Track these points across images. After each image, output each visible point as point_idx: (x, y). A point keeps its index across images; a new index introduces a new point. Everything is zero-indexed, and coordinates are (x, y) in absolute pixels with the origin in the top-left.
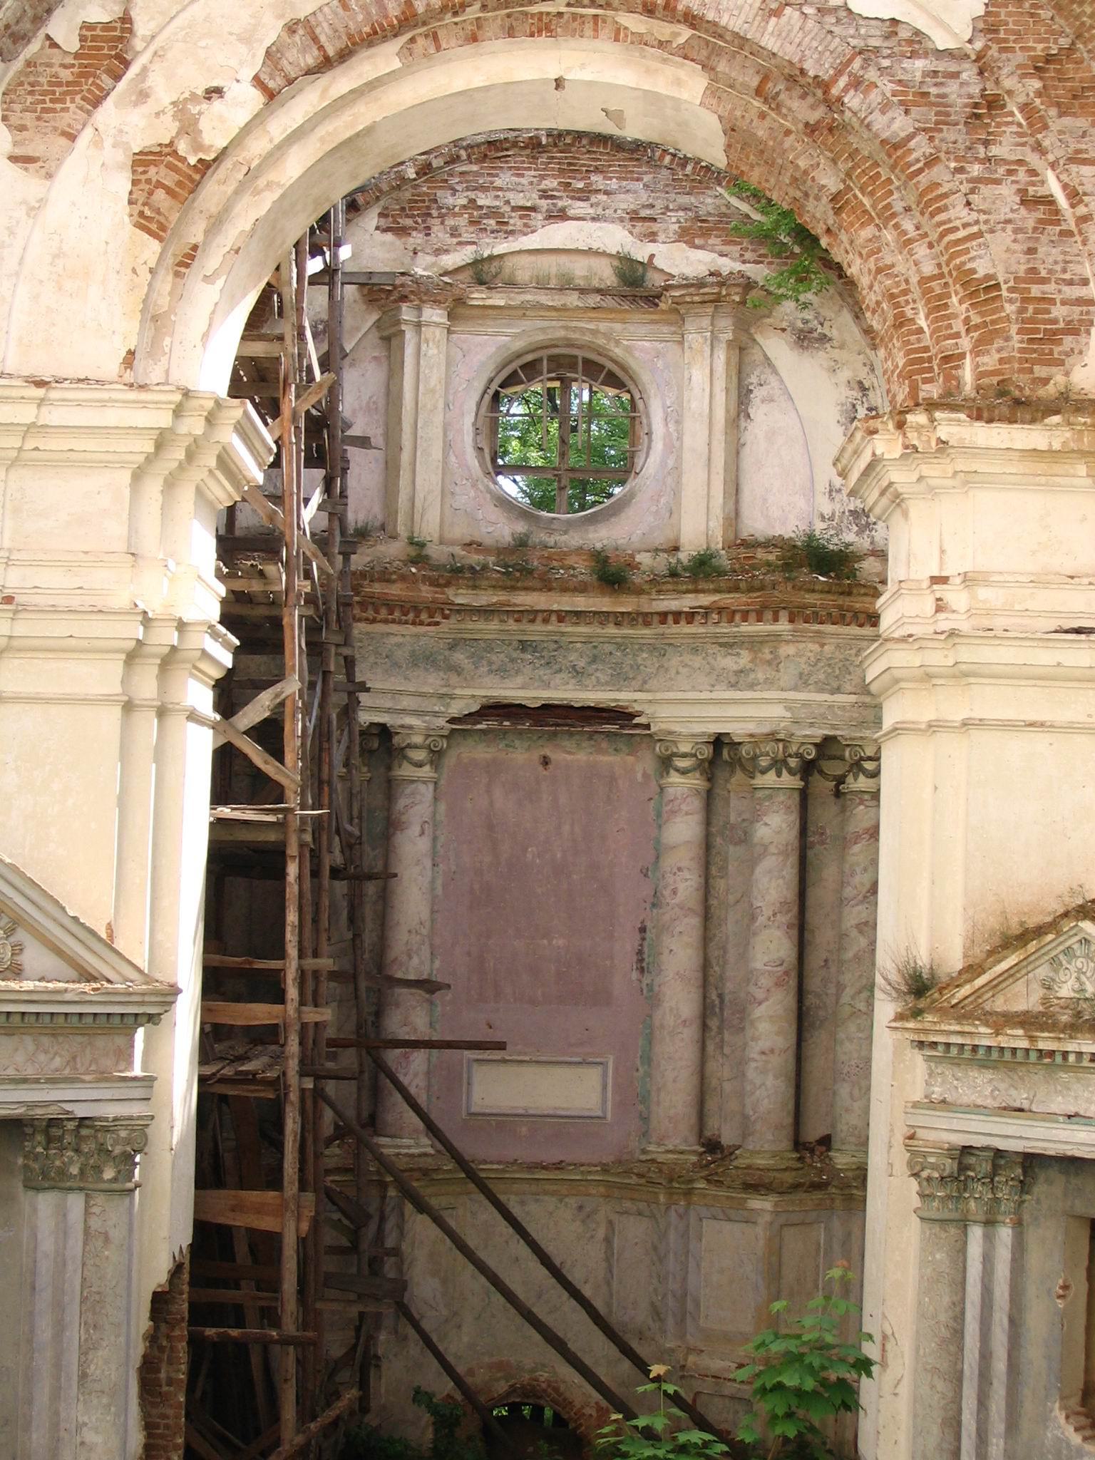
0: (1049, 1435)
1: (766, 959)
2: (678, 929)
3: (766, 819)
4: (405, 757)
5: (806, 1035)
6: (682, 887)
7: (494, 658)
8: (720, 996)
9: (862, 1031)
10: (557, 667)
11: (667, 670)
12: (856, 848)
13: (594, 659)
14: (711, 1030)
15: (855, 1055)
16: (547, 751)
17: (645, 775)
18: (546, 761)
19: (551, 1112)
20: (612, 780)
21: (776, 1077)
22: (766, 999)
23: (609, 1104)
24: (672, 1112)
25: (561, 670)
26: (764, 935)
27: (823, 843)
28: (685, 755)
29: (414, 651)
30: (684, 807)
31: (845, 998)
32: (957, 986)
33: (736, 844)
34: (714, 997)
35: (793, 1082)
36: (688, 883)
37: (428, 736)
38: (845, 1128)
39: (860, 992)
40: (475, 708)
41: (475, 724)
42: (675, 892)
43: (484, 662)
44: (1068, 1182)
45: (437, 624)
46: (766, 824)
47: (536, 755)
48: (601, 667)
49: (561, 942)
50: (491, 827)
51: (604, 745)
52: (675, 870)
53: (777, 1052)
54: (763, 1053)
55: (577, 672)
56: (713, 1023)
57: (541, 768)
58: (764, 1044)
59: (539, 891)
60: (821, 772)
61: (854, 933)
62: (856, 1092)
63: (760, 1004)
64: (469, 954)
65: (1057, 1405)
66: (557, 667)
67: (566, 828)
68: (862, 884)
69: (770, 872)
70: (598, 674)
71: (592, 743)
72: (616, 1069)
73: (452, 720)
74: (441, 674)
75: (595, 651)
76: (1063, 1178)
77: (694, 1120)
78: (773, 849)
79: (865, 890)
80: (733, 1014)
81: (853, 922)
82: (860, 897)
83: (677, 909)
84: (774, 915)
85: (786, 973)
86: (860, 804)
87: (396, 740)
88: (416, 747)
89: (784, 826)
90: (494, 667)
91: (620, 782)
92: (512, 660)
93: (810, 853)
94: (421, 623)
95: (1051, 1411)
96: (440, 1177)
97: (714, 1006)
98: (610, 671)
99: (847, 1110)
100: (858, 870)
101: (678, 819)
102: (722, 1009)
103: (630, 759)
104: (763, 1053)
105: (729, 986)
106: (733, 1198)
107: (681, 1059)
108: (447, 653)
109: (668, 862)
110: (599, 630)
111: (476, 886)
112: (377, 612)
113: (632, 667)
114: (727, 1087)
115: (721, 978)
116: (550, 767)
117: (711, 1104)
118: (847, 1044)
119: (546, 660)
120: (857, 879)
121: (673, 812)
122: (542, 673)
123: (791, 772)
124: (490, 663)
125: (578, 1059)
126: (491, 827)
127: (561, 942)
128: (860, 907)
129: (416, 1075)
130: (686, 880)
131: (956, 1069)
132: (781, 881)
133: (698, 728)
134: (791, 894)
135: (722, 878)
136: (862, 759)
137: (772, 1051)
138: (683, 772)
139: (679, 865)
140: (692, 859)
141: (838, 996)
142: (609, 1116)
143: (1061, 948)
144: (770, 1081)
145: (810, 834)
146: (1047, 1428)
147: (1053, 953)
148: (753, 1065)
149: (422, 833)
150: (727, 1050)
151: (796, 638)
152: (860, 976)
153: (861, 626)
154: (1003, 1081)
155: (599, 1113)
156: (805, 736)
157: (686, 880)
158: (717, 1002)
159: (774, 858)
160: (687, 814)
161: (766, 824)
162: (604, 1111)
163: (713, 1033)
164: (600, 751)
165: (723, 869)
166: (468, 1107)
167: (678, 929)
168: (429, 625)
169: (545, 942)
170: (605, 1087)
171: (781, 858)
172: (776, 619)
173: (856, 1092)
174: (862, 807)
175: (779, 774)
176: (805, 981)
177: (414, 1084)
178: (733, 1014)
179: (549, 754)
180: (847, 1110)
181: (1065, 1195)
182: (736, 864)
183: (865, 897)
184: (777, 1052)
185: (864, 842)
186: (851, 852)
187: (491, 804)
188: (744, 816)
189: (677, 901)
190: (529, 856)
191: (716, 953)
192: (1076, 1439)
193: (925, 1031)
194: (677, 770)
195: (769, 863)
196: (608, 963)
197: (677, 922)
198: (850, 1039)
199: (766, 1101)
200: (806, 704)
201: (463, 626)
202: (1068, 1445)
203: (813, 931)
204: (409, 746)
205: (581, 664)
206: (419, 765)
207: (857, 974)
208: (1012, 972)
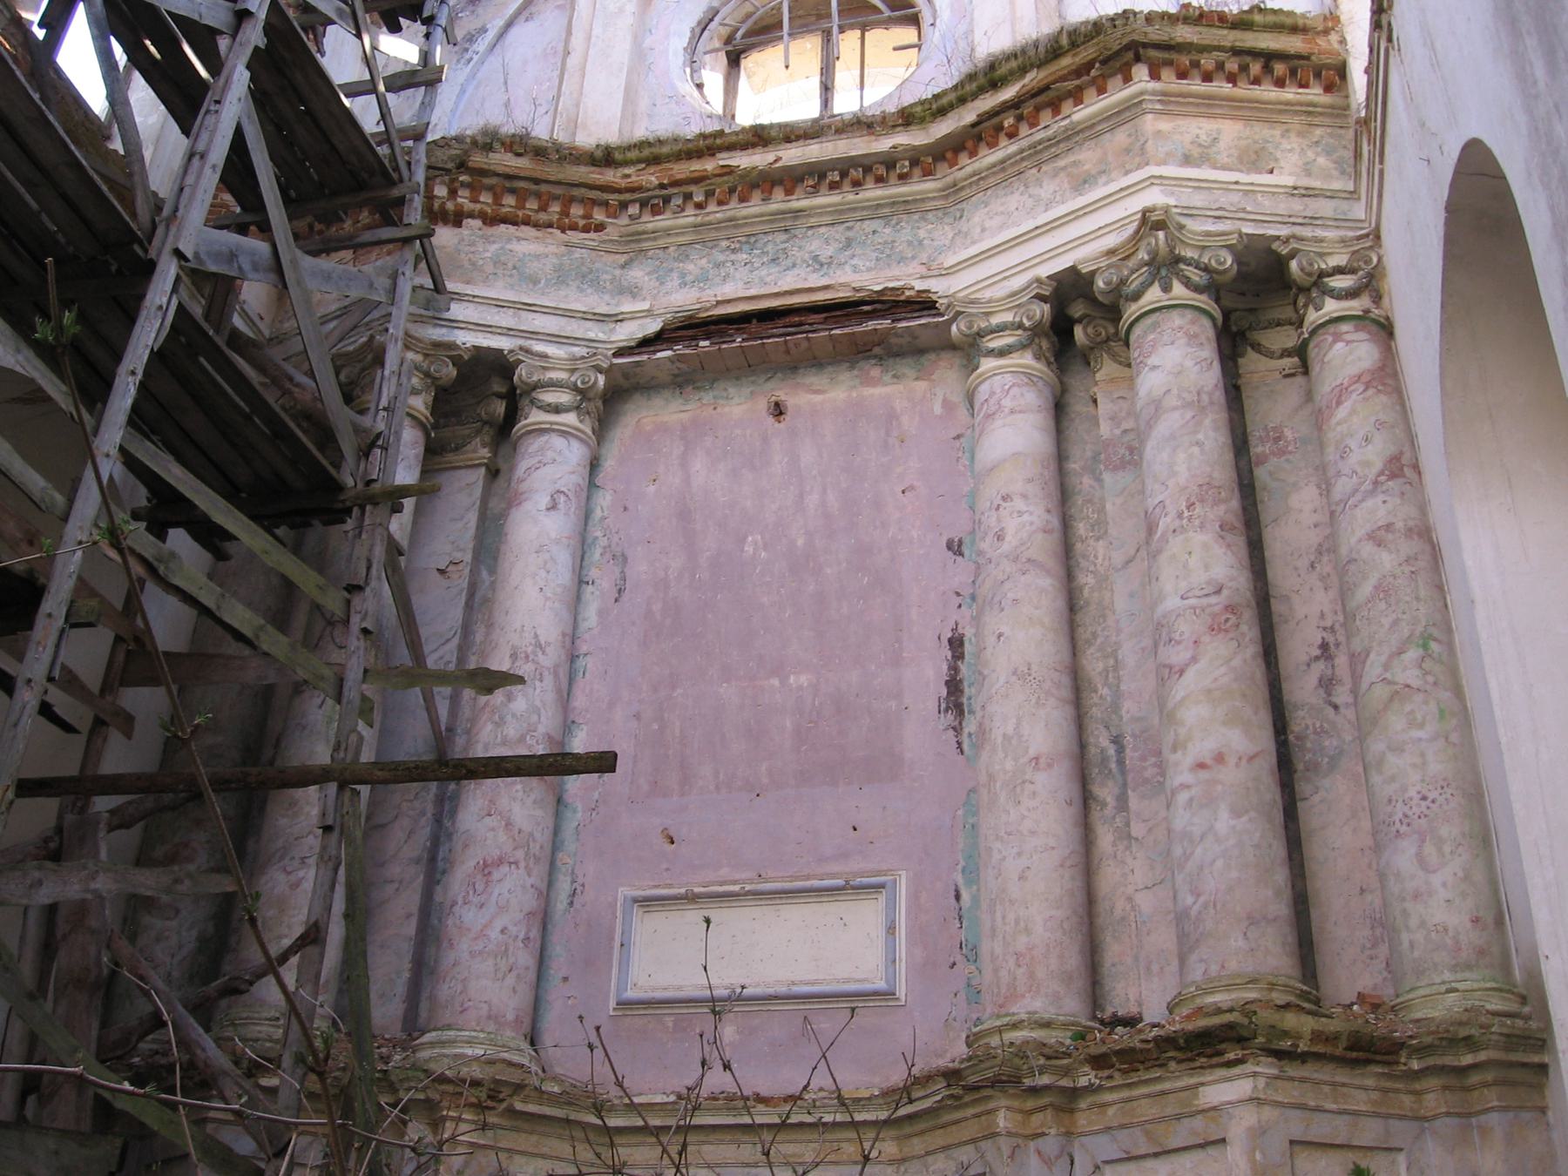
1: (1183, 585)
2: (1010, 595)
3: (1152, 361)
4: (532, 402)
5: (1303, 788)
6: (1011, 526)
7: (691, 267)
8: (1117, 741)
9: (1421, 726)
10: (789, 262)
11: (966, 234)
12: (1341, 412)
13: (849, 243)
14: (1104, 805)
15: (1415, 777)
16: (782, 395)
17: (947, 404)
18: (778, 411)
19: (783, 990)
20: (891, 417)
21: (1236, 813)
22: (1194, 659)
23: (902, 967)
24: (1021, 942)
25: (794, 265)
26: (1175, 545)
27: (1282, 452)
28: (1001, 328)
29: (562, 264)
30: (1007, 403)
31: (1373, 669)
33: (1115, 469)
34: (1104, 742)
35: (1279, 817)
36: (1026, 517)
37: (573, 371)
38: (1419, 937)
39: (1400, 652)
40: (653, 327)
41: (655, 352)
42: (1000, 537)
43: (675, 275)
45: (600, 228)
46: (1155, 368)
47: (762, 405)
48: (858, 251)
49: (804, 680)
50: (684, 515)
51: (875, 372)
52: (998, 501)
53: (1232, 761)
54: (1202, 766)
55: (818, 263)
56: (1105, 792)
57: (771, 420)
58: (1202, 747)
59: (765, 600)
60: (1257, 347)
61: (1368, 549)
62: (1429, 849)
63: (1182, 672)
64: (637, 716)
66: (789, 262)
67: (813, 500)
68: (1367, 464)
69: (1173, 437)
70: (854, 262)
71: (855, 372)
72: (914, 897)
73: (620, 353)
74: (607, 297)
75: (850, 234)
77: (1074, 960)
78: (1171, 401)
79: (1372, 473)
80: (1143, 758)
81: (1360, 533)
82: (1367, 486)
83: (1007, 567)
84: (1190, 506)
85: (1230, 608)
86: (1335, 342)
87: (522, 373)
88: (553, 384)
89: (1189, 363)
90: (689, 278)
91: (905, 420)
92: (718, 265)
93: (1261, 473)
94: (574, 227)
96: (532, 1108)
97: (1105, 760)
98: (874, 255)
99: (1417, 896)
100: (1353, 444)
101: (998, 423)
102: (1121, 762)
103: (921, 386)
104: (1202, 766)
105: (1129, 708)
106: (1163, 1093)
107: (1033, 833)
108: (618, 272)
109: (990, 492)
110: (851, 197)
111: (657, 607)
112: (497, 201)
113: (910, 243)
114: (1145, 902)
115: (1115, 707)
116: (787, 417)
117: (1114, 951)
118: (1392, 760)
119: (770, 257)
120: (1353, 459)
121: (989, 416)
122: (764, 273)
123: (1187, 283)
124: (683, 275)
125: (840, 882)
126: (684, 515)
127: (804, 680)
128: (1369, 503)
129: (502, 909)
130: (1020, 513)
132: (1196, 450)
133: (1018, 282)
134: (1223, 474)
135: (1098, 539)
136: (1322, 274)
137: (1220, 758)
138: (1002, 353)
139: (1004, 491)
140: (1030, 481)
141: (1356, 677)
142: (901, 992)
144: (1224, 821)
145: (1253, 441)
148: (1182, 797)
149: (553, 507)
150: (1137, 829)
151: (1171, 104)
152: (1396, 622)
153: (1280, 83)
155: (881, 985)
156: (1208, 234)
157: (1020, 513)
158: (1111, 751)
159: (1176, 415)
160: (1012, 412)
161: (1155, 368)
162: (891, 977)
163: (1109, 811)
164: (870, 382)
165: (1100, 527)
166: (622, 984)
167: (1010, 595)
168: (586, 229)
169: (776, 682)
170: (891, 929)
171: (1189, 415)
172: (1128, 79)
173: (1429, 849)
174: (1340, 345)
175: (1167, 289)
176: (1285, 686)
177: (498, 924)
178: (1143, 758)
179: (783, 398)
180: (1417, 896)
182: (1119, 501)
183: (1376, 483)
184: (1232, 761)
185: (1354, 396)
186: (1334, 421)
187: (687, 480)
188: (1125, 426)
189: (1006, 547)
190: (749, 549)
191: (1100, 666)
194: (991, 353)
195: (1170, 423)
196: (893, 704)
197: (1007, 585)
198: (1398, 749)
199: (1219, 863)
200: (1199, 185)
201: (640, 228)
203: (1287, 598)
204: (537, 386)
205: (827, 252)
206: (557, 409)
207: (1386, 622)
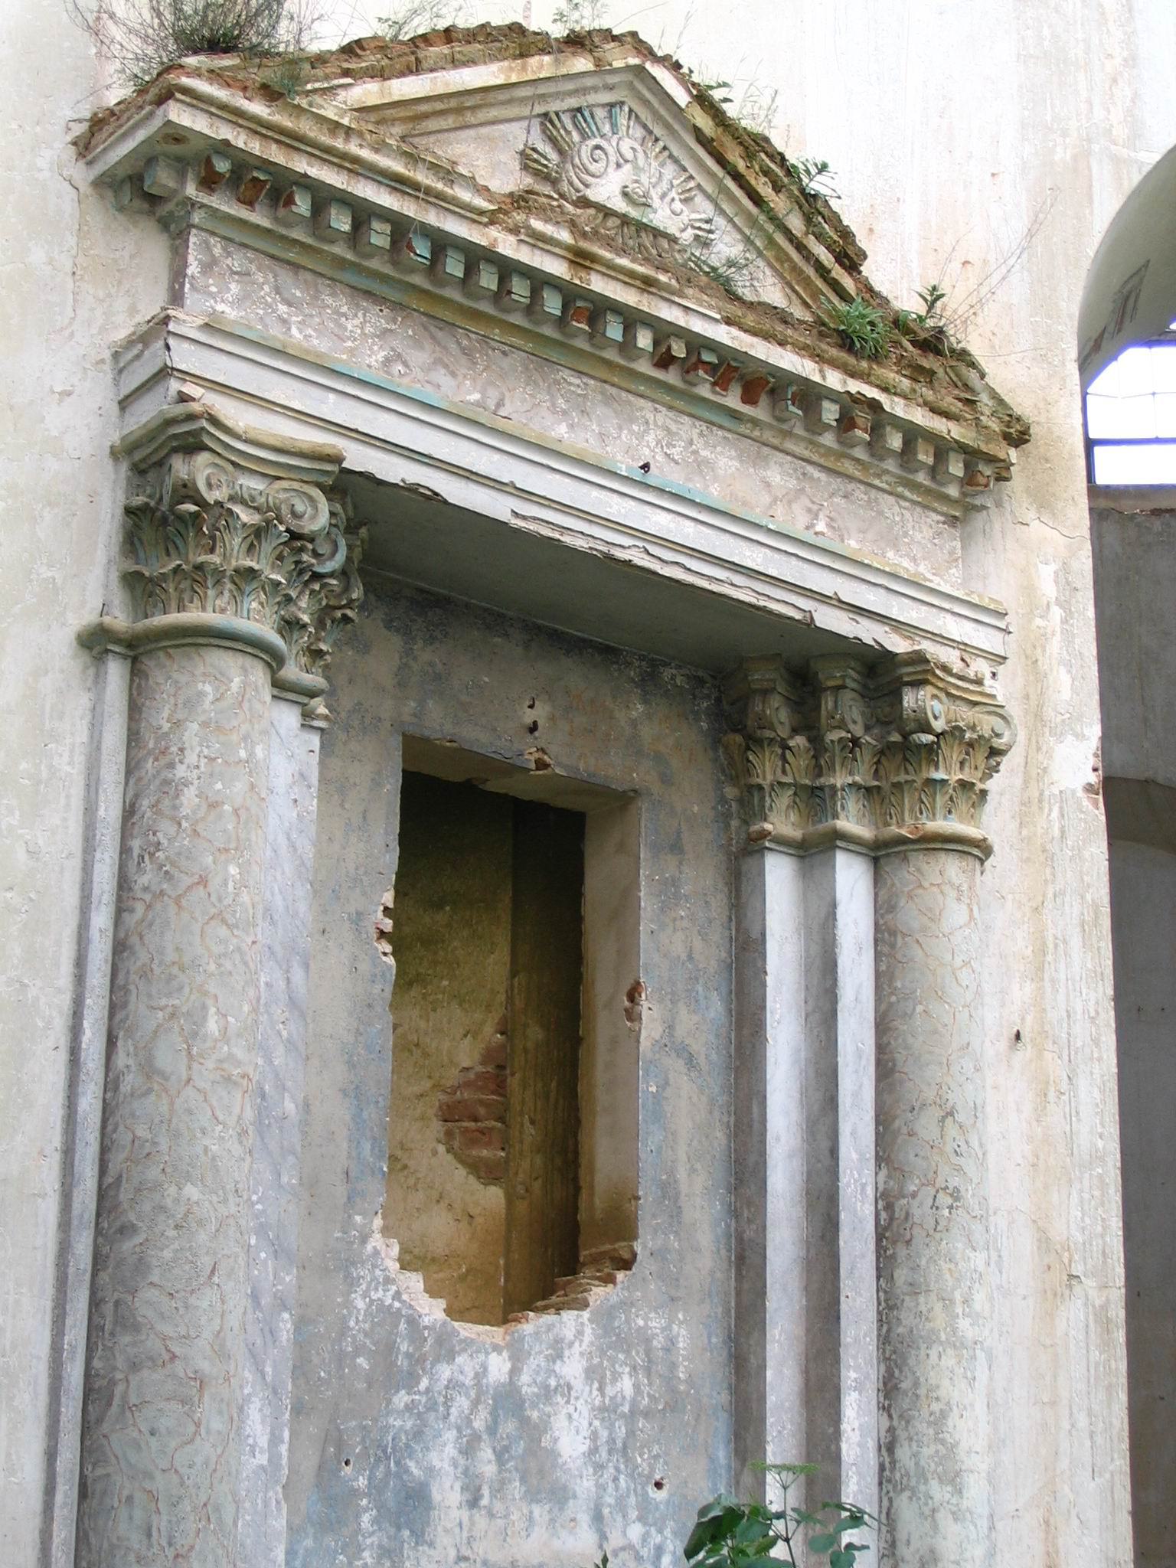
0: (360, 1304)
32: (346, 73)
44: (408, 652)
65: (378, 1222)
76: (397, 641)
95: (364, 1239)
131: (285, 276)
143: (573, 102)
146: (351, 1283)
147: (554, 106)
154: (418, 344)
181: (401, 685)
192: (432, 1311)
193: (293, 141)
202: (413, 1322)
208: (542, 89)
